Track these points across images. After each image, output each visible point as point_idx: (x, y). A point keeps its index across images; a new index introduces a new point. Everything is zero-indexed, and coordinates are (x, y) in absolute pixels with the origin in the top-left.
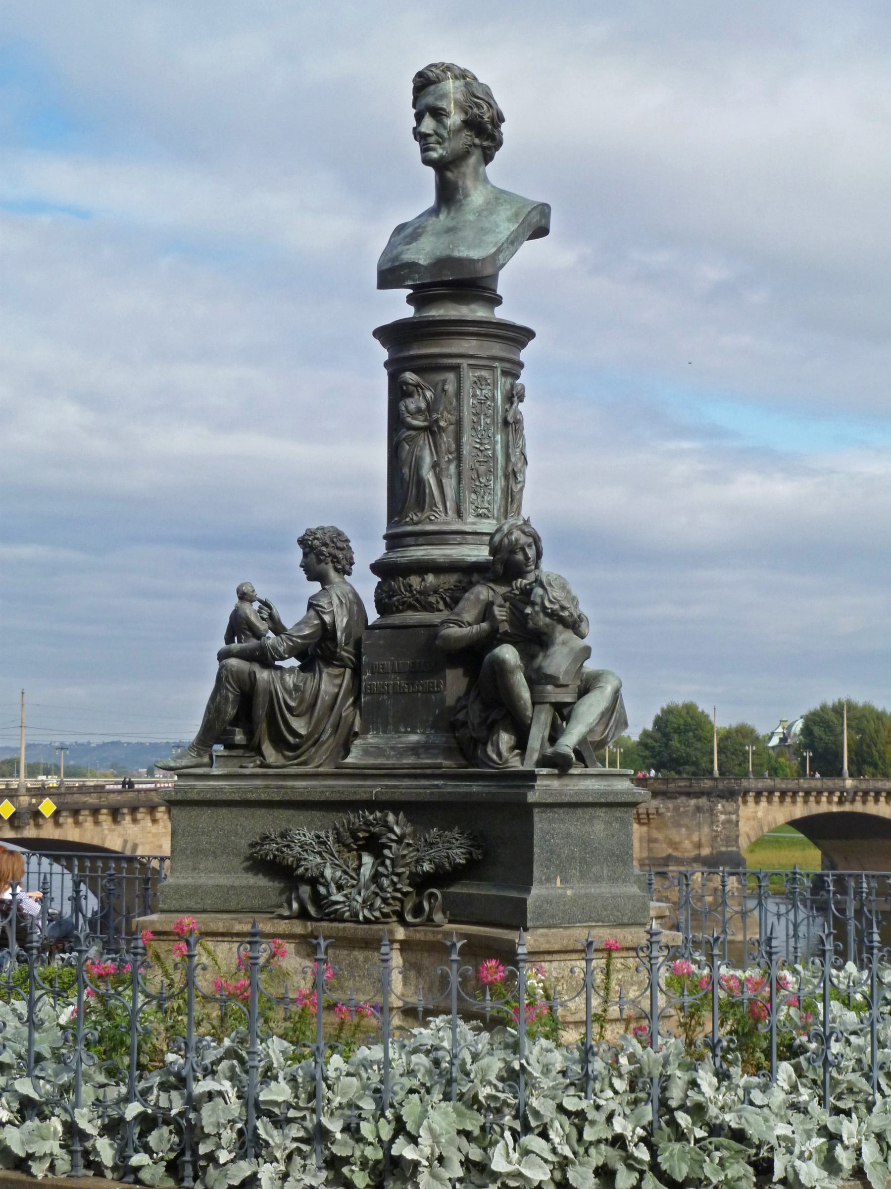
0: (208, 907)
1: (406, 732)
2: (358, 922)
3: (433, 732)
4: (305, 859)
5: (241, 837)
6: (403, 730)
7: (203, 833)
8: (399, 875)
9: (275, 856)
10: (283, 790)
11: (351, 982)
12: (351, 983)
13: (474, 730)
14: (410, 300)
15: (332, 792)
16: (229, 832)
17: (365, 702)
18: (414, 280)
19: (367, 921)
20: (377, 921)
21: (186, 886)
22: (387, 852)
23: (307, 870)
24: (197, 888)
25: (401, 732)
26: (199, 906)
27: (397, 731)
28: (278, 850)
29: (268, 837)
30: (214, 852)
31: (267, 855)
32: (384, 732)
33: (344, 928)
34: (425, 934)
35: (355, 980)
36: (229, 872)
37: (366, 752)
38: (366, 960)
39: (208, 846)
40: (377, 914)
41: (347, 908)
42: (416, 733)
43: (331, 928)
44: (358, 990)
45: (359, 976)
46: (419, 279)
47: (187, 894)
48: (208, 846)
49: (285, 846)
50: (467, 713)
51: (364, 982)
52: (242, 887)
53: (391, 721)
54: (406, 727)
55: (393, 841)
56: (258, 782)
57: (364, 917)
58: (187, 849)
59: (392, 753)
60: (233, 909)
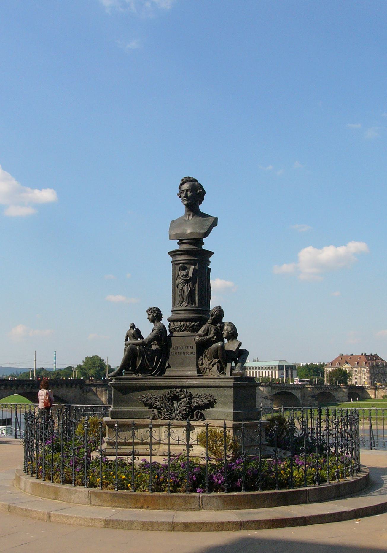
13: (206, 365)
14: (178, 243)
20: (181, 420)
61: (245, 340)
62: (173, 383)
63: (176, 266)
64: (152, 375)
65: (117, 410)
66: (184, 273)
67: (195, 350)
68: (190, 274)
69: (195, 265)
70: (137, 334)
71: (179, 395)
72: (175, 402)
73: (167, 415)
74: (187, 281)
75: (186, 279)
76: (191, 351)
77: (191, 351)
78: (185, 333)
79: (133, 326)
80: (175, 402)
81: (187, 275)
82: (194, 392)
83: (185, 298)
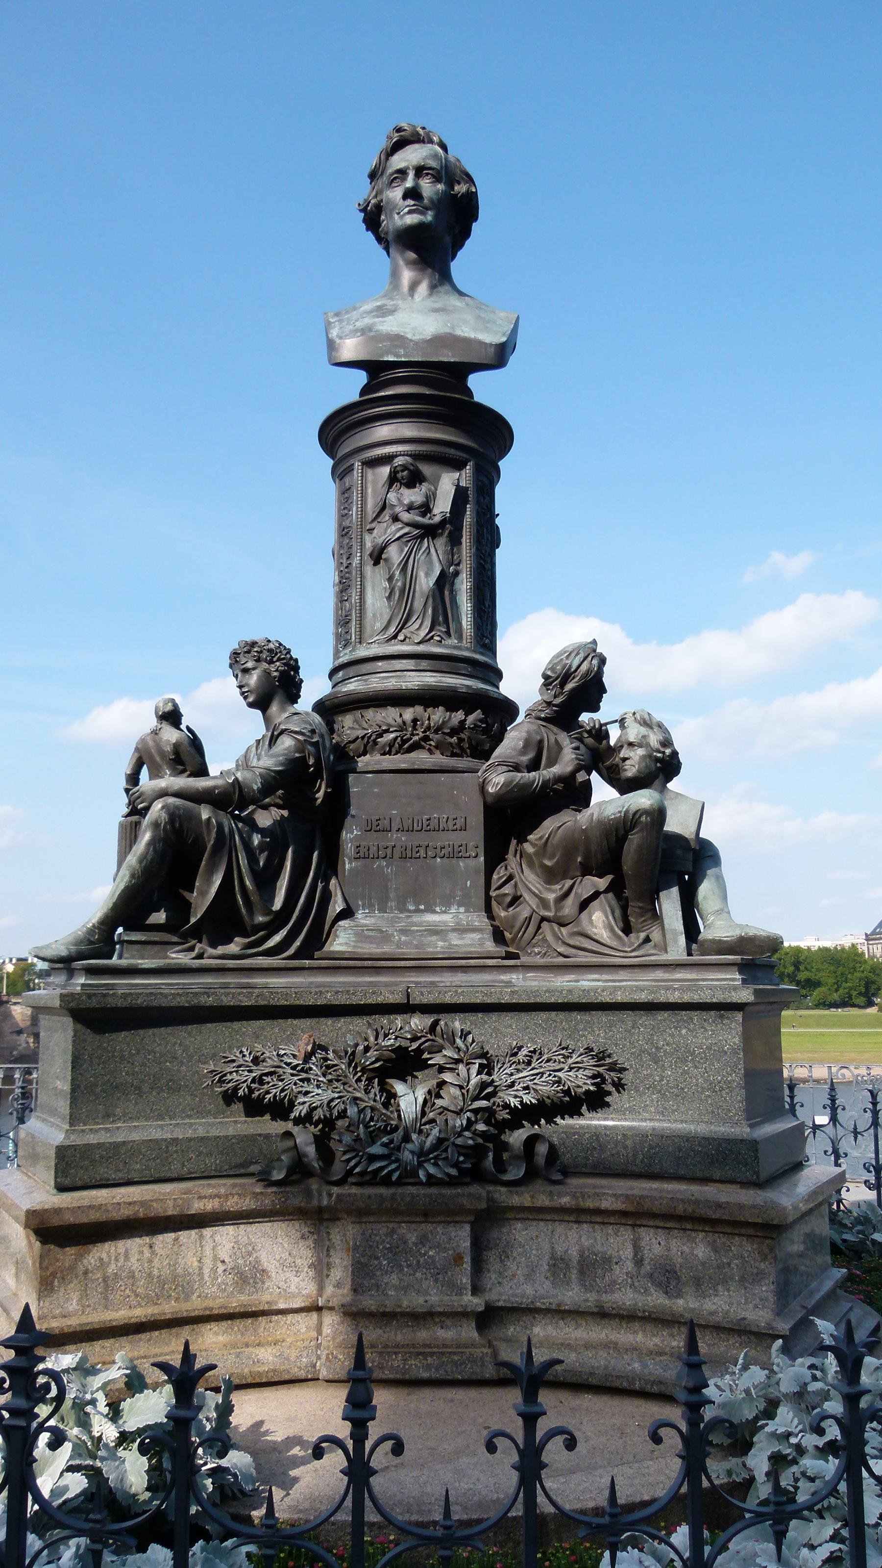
0: (136, 1177)
1: (417, 911)
2: (421, 1183)
3: (462, 910)
4: (307, 1093)
5: (182, 1063)
6: (412, 908)
7: (122, 1058)
8: (476, 1111)
9: (251, 1091)
10: (256, 991)
11: (394, 1276)
12: (394, 1279)
15: (337, 992)
16: (162, 1055)
17: (351, 869)
18: (397, 356)
19: (432, 1181)
20: (451, 1182)
21: (100, 1145)
22: (447, 1077)
23: (312, 1109)
24: (117, 1146)
25: (409, 911)
26: (120, 1175)
27: (402, 909)
28: (253, 1081)
29: (233, 1061)
30: (139, 1088)
31: (236, 1089)
32: (383, 910)
33: (393, 1197)
34: (532, 1197)
35: (401, 1271)
36: (161, 1117)
37: (361, 936)
38: (423, 1240)
39: (129, 1079)
40: (453, 1172)
41: (393, 1166)
42: (434, 912)
43: (369, 1197)
44: (406, 1289)
45: (409, 1266)
46: (404, 356)
47: (102, 1157)
48: (129, 1079)
49: (267, 1074)
50: (516, 885)
51: (418, 1275)
52: (190, 1140)
53: (392, 895)
54: (417, 904)
55: (458, 1061)
56: (209, 980)
57: (429, 1176)
58: (95, 1085)
59: (403, 938)
60: (175, 1175)
61: (705, 802)
62: (387, 988)
63: (370, 473)
64: (270, 953)
65: (92, 1139)
66: (413, 496)
67: (474, 837)
68: (443, 506)
69: (457, 465)
70: (189, 756)
71: (419, 1051)
72: (399, 1087)
73: (373, 1158)
74: (430, 532)
75: (425, 521)
76: (455, 839)
77: (455, 839)
78: (421, 758)
79: (172, 717)
80: (399, 1087)
81: (425, 508)
82: (497, 1034)
83: (418, 604)
